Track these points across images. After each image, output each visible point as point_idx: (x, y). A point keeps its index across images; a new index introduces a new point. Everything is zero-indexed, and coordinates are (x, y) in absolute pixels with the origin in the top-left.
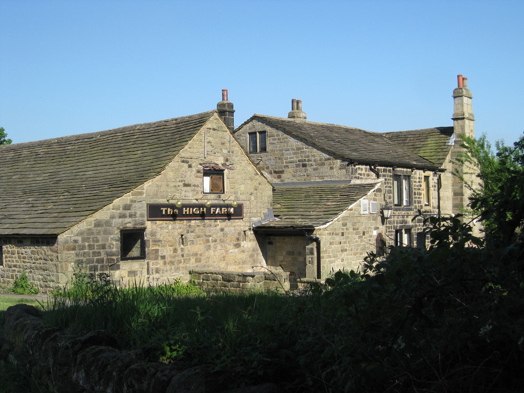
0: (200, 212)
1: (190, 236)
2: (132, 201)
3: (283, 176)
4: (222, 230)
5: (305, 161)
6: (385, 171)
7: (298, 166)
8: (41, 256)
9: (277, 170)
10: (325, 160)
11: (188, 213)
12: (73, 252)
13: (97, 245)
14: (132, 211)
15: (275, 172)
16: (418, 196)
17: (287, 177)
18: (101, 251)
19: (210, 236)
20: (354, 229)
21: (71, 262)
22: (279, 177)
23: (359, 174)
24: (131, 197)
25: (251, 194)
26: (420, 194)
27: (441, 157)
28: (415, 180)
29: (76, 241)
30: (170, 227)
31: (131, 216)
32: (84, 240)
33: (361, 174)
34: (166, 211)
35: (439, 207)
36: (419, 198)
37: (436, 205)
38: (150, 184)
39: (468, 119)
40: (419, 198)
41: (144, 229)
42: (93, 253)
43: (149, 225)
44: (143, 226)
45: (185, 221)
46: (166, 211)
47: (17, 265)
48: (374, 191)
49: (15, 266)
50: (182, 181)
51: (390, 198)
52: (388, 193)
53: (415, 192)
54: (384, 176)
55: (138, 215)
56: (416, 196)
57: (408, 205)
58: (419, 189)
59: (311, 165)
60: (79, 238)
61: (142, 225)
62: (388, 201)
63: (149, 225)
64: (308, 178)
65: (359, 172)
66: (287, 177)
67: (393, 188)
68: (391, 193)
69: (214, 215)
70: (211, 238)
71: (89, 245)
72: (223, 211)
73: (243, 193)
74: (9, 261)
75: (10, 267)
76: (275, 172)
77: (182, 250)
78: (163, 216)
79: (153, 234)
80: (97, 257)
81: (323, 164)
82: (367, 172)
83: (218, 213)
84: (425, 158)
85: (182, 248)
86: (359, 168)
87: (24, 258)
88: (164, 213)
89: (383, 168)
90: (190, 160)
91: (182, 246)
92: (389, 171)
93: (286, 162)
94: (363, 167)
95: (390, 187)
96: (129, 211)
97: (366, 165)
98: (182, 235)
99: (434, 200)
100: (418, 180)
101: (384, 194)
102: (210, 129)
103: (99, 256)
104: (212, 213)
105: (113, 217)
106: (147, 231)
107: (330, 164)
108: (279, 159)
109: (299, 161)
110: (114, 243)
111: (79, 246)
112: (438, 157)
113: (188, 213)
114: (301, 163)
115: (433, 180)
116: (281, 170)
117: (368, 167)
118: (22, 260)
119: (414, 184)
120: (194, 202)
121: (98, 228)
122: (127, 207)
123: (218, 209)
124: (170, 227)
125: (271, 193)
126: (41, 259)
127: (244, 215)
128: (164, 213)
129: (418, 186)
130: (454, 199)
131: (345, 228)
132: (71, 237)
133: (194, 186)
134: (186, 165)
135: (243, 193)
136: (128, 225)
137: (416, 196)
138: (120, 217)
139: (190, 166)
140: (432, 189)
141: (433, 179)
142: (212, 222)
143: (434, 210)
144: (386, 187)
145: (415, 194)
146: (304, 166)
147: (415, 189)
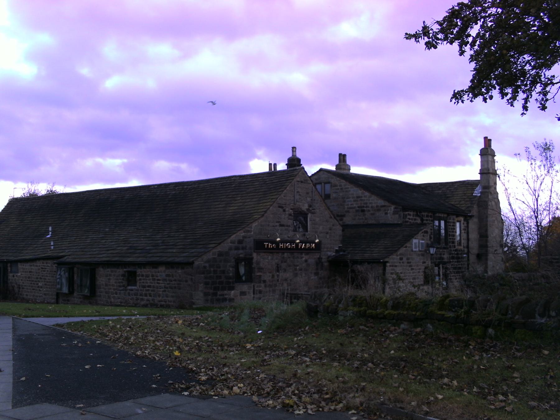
0: (291, 247)
1: (284, 265)
5: (364, 207)
9: (339, 214)
16: (452, 237)
34: (268, 245)
40: (453, 239)
43: (255, 255)
44: (251, 257)
47: (151, 286)
48: (422, 233)
53: (450, 234)
63: (255, 255)
72: (307, 246)
77: (278, 276)
79: (258, 263)
82: (415, 217)
87: (158, 280)
93: (348, 208)
98: (278, 264)
104: (299, 247)
114: (360, 209)
118: (156, 281)
123: (304, 245)
124: (270, 257)
129: (452, 229)
131: (402, 261)
134: (281, 210)
146: (363, 211)
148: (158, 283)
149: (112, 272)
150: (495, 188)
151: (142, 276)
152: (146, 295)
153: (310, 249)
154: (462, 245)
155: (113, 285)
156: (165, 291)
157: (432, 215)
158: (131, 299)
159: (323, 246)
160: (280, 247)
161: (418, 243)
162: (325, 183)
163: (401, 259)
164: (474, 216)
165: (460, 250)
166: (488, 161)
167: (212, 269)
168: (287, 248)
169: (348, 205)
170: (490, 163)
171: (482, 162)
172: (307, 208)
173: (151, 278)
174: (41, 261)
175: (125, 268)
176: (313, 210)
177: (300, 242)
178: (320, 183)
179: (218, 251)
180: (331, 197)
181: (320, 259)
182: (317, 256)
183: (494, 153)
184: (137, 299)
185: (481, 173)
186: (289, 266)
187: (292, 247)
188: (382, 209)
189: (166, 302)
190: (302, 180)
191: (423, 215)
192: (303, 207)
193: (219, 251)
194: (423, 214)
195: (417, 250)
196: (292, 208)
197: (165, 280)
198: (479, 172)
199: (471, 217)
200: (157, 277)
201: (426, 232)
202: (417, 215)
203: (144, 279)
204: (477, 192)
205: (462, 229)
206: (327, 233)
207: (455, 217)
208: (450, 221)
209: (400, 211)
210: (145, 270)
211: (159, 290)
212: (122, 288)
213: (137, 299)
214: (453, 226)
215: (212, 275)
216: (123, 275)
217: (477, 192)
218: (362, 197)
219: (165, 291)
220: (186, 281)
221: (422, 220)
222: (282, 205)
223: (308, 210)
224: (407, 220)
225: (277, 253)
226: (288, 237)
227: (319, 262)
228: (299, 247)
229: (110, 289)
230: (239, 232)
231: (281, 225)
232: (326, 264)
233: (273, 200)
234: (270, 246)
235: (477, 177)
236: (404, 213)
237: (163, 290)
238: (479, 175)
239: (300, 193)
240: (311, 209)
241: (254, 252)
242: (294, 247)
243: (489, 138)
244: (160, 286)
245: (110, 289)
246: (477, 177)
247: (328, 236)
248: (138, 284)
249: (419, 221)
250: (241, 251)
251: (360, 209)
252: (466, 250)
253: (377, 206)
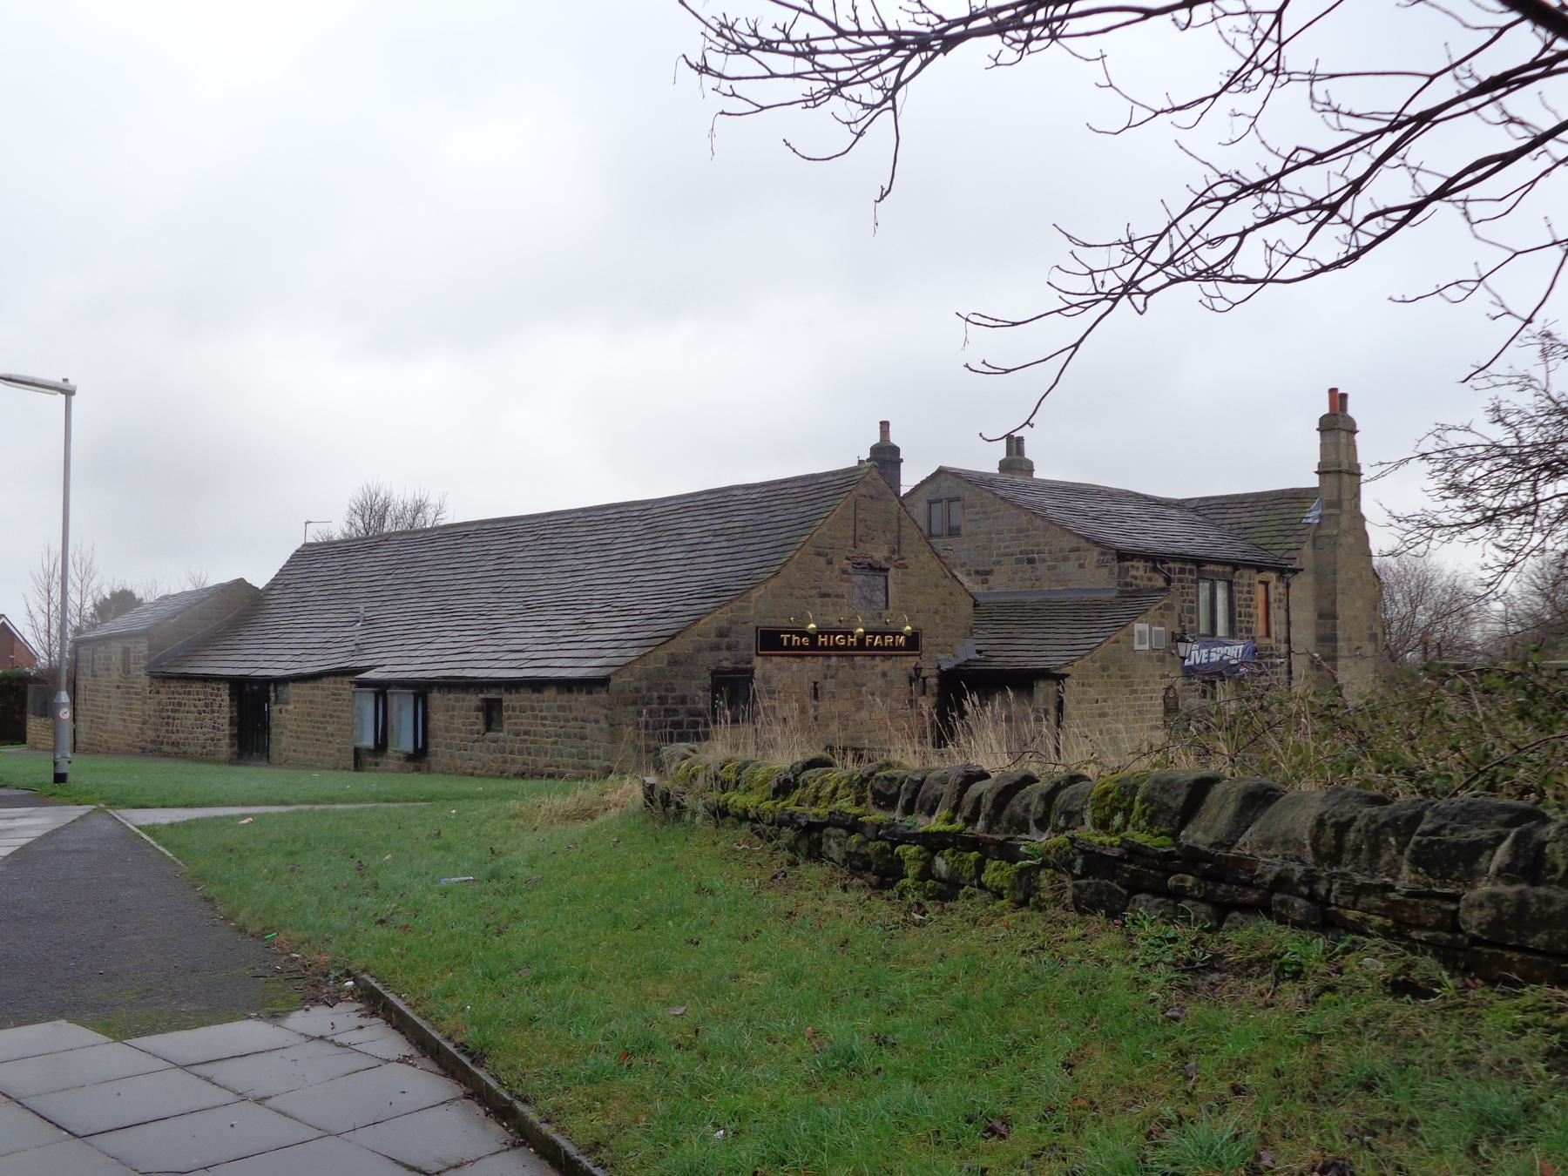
0: (846, 642)
1: (829, 685)
2: (731, 622)
3: (991, 578)
4: (884, 675)
6: (1182, 571)
7: (1019, 561)
8: (575, 714)
9: (981, 569)
10: (1071, 551)
11: (826, 644)
12: (631, 708)
13: (673, 698)
14: (732, 639)
15: (977, 572)
16: (1247, 619)
17: (998, 582)
18: (679, 707)
19: (864, 685)
20: (1122, 677)
21: (628, 726)
22: (985, 582)
23: (1132, 577)
24: (730, 614)
25: (936, 612)
26: (1251, 616)
27: (1293, 546)
28: (1240, 588)
29: (637, 690)
30: (795, 667)
31: (729, 648)
32: (649, 689)
33: (1136, 578)
34: (790, 640)
35: (1288, 641)
36: (1248, 622)
37: (1283, 635)
38: (761, 592)
39: (1348, 473)
40: (1248, 622)
41: (752, 671)
42: (666, 710)
43: (758, 662)
45: (821, 658)
46: (790, 640)
48: (1160, 608)
49: (526, 733)
50: (816, 588)
51: (1191, 621)
52: (1188, 613)
53: (1240, 612)
54: (1180, 580)
55: (741, 647)
56: (1242, 618)
57: (1209, 633)
58: (1249, 606)
59: (1044, 561)
60: (644, 684)
61: (748, 663)
62: (1188, 626)
63: (758, 662)
64: (1037, 584)
65: (1133, 572)
66: (998, 582)
67: (1198, 604)
68: (1193, 613)
69: (871, 648)
70: (864, 689)
71: (660, 698)
72: (886, 641)
73: (922, 611)
74: (515, 724)
76: (977, 572)
77: (816, 708)
78: (781, 647)
80: (672, 718)
81: (1065, 559)
83: (878, 645)
85: (814, 706)
86: (1132, 566)
87: (543, 718)
88: (785, 643)
89: (1178, 566)
90: (829, 551)
91: (815, 702)
92: (1191, 572)
93: (998, 555)
94: (1141, 564)
95: (1193, 602)
96: (728, 639)
97: (1147, 561)
98: (815, 683)
99: (1278, 627)
100: (1246, 589)
101: (1179, 615)
102: (865, 496)
103: (675, 715)
106: (758, 673)
108: (985, 549)
109: (1021, 553)
111: (644, 698)
112: (1288, 546)
113: (826, 644)
114: (1025, 557)
115: (1276, 589)
116: (987, 568)
117: (1150, 564)
119: (1238, 595)
120: (837, 624)
121: (674, 668)
122: (722, 633)
123: (877, 637)
124: (795, 667)
125: (970, 609)
126: (575, 719)
128: (785, 643)
129: (1245, 600)
130: (1318, 625)
132: (630, 682)
133: (837, 596)
134: (822, 560)
135: (922, 611)
136: (725, 664)
137: (1242, 618)
138: (711, 649)
139: (829, 562)
140: (1273, 606)
141: (1276, 588)
142: (868, 662)
143: (1278, 644)
144: (1184, 601)
145: (1240, 616)
146: (1031, 561)
147: (1240, 606)
148: (544, 725)
149: (457, 700)
150: (1358, 506)
151: (514, 709)
152: (521, 753)
153: (893, 647)
154: (1273, 635)
155: (459, 731)
156: (555, 743)
157: (1194, 567)
158: (493, 761)
159: (924, 641)
160: (820, 644)
161: (1147, 632)
162: (951, 500)
163: (1104, 668)
164: (1302, 570)
165: (1266, 648)
166: (1337, 445)
167: (655, 694)
168: (836, 647)
169: (999, 547)
170: (1343, 448)
171: (1322, 445)
173: (529, 713)
174: (332, 679)
175: (481, 692)
177: (866, 633)
178: (941, 501)
179: (668, 655)
180: (963, 531)
181: (917, 669)
182: (910, 662)
183: (1354, 424)
184: (505, 762)
185: (1321, 472)
186: (844, 685)
187: (849, 644)
188: (1074, 555)
189: (558, 767)
190: (873, 493)
191: (1169, 570)
192: (875, 554)
193: (672, 654)
194: (1171, 565)
195: (1147, 647)
196: (850, 555)
197: (555, 718)
198: (1316, 470)
199: (1295, 571)
200: (541, 711)
201: (1169, 607)
202: (1155, 569)
203: (517, 717)
204: (1312, 517)
205: (1272, 600)
206: (936, 612)
207: (1253, 572)
208: (1241, 581)
209: (1113, 559)
210: (517, 696)
211: (545, 739)
212: (476, 736)
213: (505, 762)
214: (1249, 592)
215: (655, 706)
216: (478, 709)
217: (1312, 517)
218: (1028, 530)
219: (555, 743)
220: (597, 722)
221: (1168, 581)
223: (888, 559)
224: (1129, 580)
225: (813, 656)
226: (840, 621)
227: (915, 676)
229: (454, 738)
230: (720, 611)
232: (933, 681)
233: (804, 538)
235: (1313, 481)
236: (1121, 564)
237: (553, 739)
238: (1317, 476)
239: (868, 523)
240: (895, 557)
241: (758, 655)
242: (855, 644)
243: (1340, 391)
244: (546, 732)
245: (454, 738)
246: (1313, 481)
247: (938, 619)
248: (505, 726)
249: (1160, 583)
250: (725, 654)
251: (1025, 557)
252: (1283, 648)
253: (1061, 550)
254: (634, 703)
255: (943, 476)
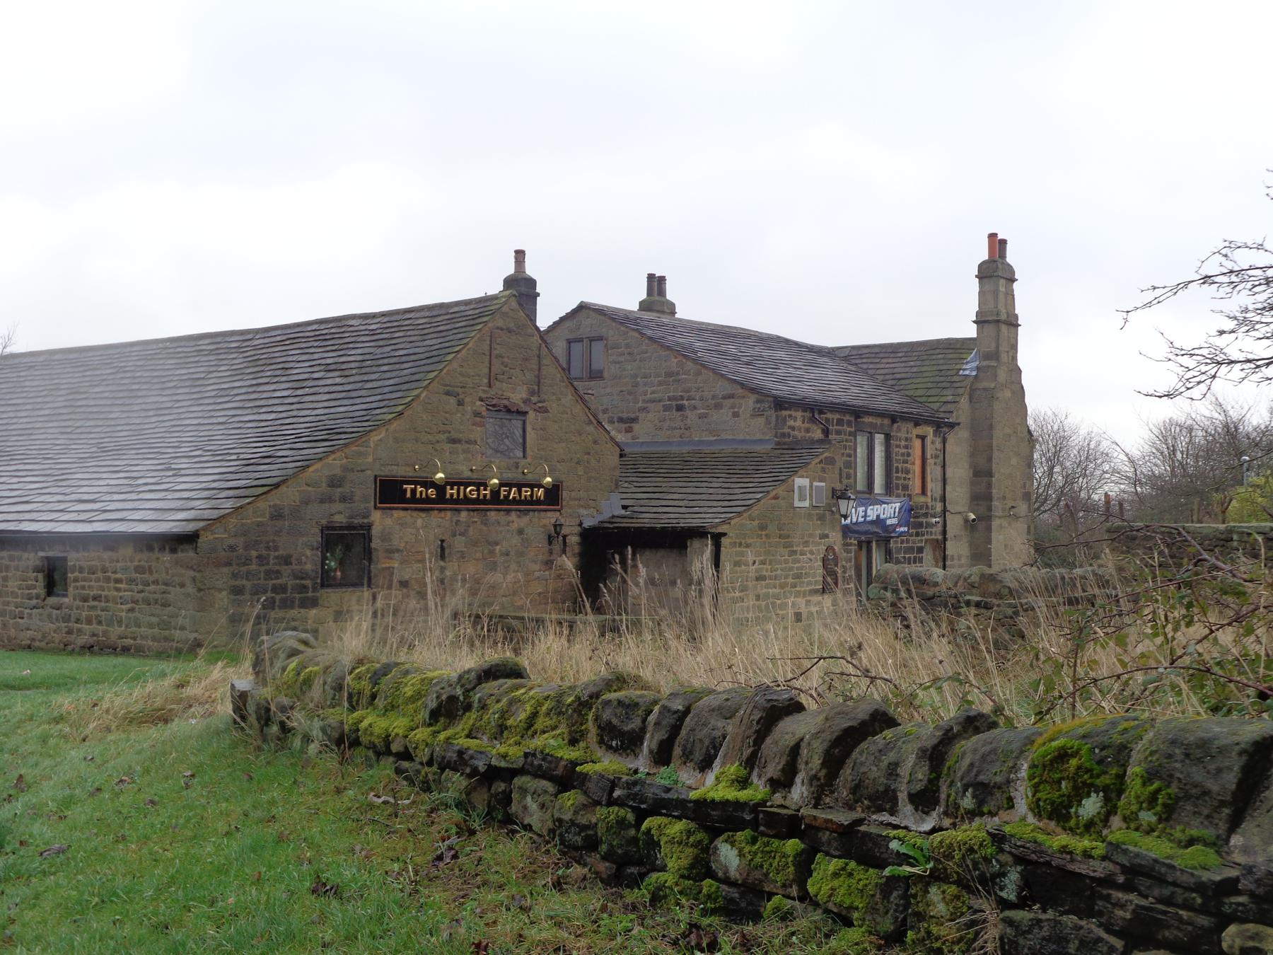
0: (478, 495)
1: (459, 543)
2: (345, 469)
3: (636, 427)
5: (682, 398)
6: (840, 422)
7: (667, 408)
8: (156, 576)
9: (625, 415)
10: (724, 398)
11: (455, 496)
12: (225, 570)
13: (277, 557)
14: (346, 489)
15: (621, 420)
17: (644, 431)
19: (497, 544)
21: (220, 590)
22: (629, 430)
24: (345, 461)
25: (578, 463)
26: (907, 472)
27: (950, 398)
29: (232, 548)
31: (344, 499)
32: (247, 547)
33: (793, 428)
34: (414, 491)
35: (943, 499)
40: (905, 479)
44: (366, 521)
45: (449, 513)
46: (414, 491)
47: (100, 596)
48: (821, 462)
49: (95, 598)
50: (444, 432)
53: (897, 468)
54: (838, 433)
55: (356, 498)
56: (899, 475)
59: (695, 408)
60: (240, 542)
61: (364, 517)
63: (376, 517)
64: (687, 433)
65: (791, 423)
66: (644, 431)
71: (259, 557)
72: (524, 494)
73: (563, 460)
74: (83, 588)
75: (85, 599)
76: (621, 420)
78: (403, 499)
79: (386, 537)
80: (274, 582)
81: (718, 406)
82: (806, 425)
83: (514, 498)
84: (919, 399)
87: (118, 581)
88: (408, 495)
89: (837, 416)
90: (460, 390)
91: (442, 563)
92: (849, 424)
93: (644, 401)
94: (799, 414)
95: (849, 456)
96: (340, 490)
97: (804, 411)
98: (442, 541)
99: (934, 485)
100: (903, 443)
102: (502, 329)
103: (277, 578)
104: (502, 497)
105: (306, 502)
106: (375, 531)
107: (733, 407)
108: (630, 393)
109: (670, 399)
110: (309, 553)
112: (943, 399)
113: (455, 496)
114: (674, 403)
116: (632, 416)
117: (808, 414)
118: (112, 585)
120: (467, 474)
122: (334, 482)
124: (419, 521)
125: (615, 460)
126: (156, 582)
127: (564, 503)
128: (408, 495)
129: (903, 455)
130: (972, 484)
132: (223, 539)
134: (452, 400)
135: (563, 460)
137: (899, 475)
138: (322, 501)
139: (460, 403)
140: (930, 461)
142: (502, 517)
146: (680, 408)
148: (118, 590)
149: (12, 558)
150: (1014, 358)
151: (81, 570)
152: (89, 622)
153: (531, 501)
154: (929, 494)
155: (14, 595)
156: (132, 610)
157: (852, 419)
158: (55, 632)
159: (565, 494)
160: (448, 496)
162: (592, 340)
163: (763, 527)
164: (959, 424)
165: (922, 508)
166: (996, 293)
167: (254, 553)
168: (467, 500)
169: (645, 393)
170: (1001, 297)
171: (982, 294)
172: (524, 396)
173: (100, 575)
175: (43, 550)
176: (540, 402)
177: (501, 485)
178: (581, 340)
180: (606, 375)
181: (557, 526)
182: (550, 518)
183: (1013, 272)
184: (69, 632)
185: (981, 321)
186: (475, 543)
187: (481, 497)
189: (135, 639)
190: (512, 325)
191: (827, 420)
192: (512, 396)
193: (275, 506)
194: (829, 416)
196: (484, 396)
197: (131, 581)
198: (975, 319)
199: (952, 426)
200: (115, 572)
201: (830, 461)
202: (813, 420)
203: (84, 580)
204: (969, 368)
205: (929, 456)
207: (910, 425)
208: (899, 434)
209: (770, 408)
210: (86, 554)
211: (119, 606)
212: (34, 602)
213: (69, 632)
214: (906, 447)
215: (253, 567)
216: (37, 570)
217: (969, 368)
218: (678, 374)
219: (132, 610)
220: (182, 585)
221: (826, 432)
222: (456, 389)
223: (526, 401)
224: (786, 430)
225: (440, 510)
226: (471, 470)
227: (555, 536)
228: (502, 497)
229: (8, 604)
230: (333, 456)
231: (454, 441)
232: (574, 540)
233: (432, 375)
234: (421, 492)
235: (971, 331)
236: (779, 413)
237: (129, 606)
238: (975, 326)
239: (506, 360)
240: (534, 399)
241: (375, 508)
242: (488, 497)
243: (1000, 237)
244: (121, 598)
245: (8, 604)
246: (971, 331)
247: (580, 470)
248: (71, 589)
249: (818, 434)
251: (674, 403)
252: (939, 507)
253: (714, 397)
254: (229, 564)
255: (584, 312)
